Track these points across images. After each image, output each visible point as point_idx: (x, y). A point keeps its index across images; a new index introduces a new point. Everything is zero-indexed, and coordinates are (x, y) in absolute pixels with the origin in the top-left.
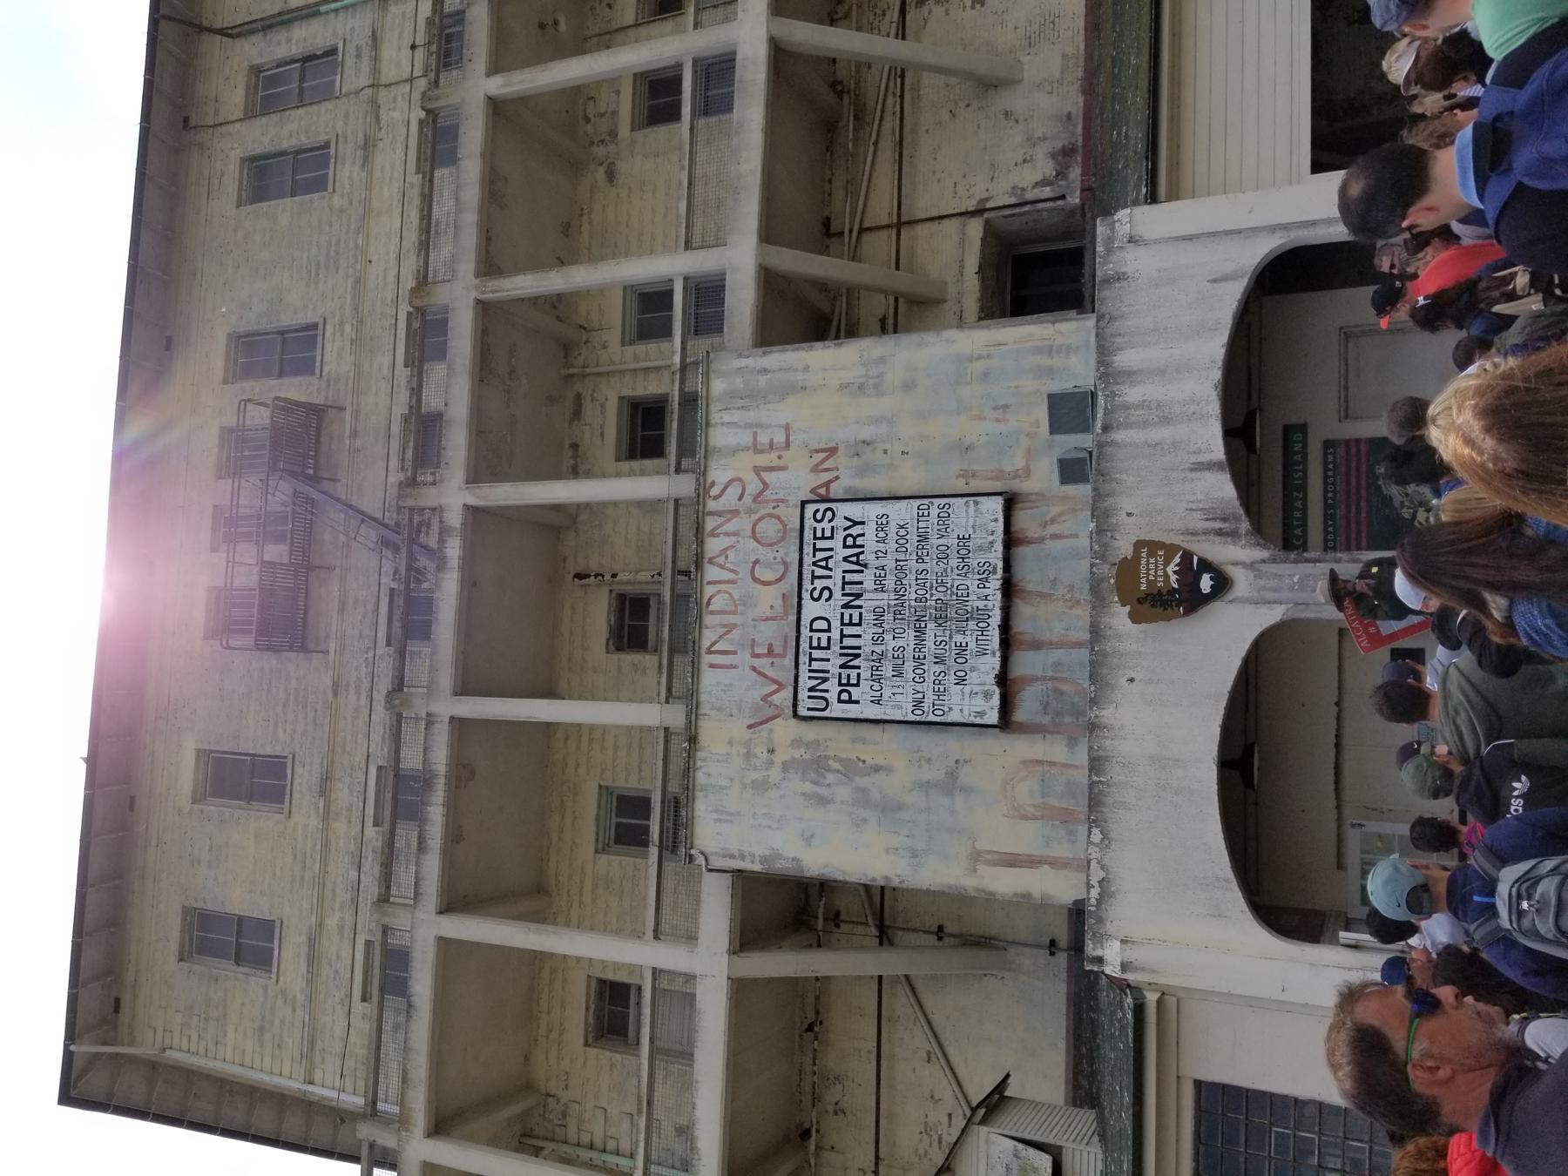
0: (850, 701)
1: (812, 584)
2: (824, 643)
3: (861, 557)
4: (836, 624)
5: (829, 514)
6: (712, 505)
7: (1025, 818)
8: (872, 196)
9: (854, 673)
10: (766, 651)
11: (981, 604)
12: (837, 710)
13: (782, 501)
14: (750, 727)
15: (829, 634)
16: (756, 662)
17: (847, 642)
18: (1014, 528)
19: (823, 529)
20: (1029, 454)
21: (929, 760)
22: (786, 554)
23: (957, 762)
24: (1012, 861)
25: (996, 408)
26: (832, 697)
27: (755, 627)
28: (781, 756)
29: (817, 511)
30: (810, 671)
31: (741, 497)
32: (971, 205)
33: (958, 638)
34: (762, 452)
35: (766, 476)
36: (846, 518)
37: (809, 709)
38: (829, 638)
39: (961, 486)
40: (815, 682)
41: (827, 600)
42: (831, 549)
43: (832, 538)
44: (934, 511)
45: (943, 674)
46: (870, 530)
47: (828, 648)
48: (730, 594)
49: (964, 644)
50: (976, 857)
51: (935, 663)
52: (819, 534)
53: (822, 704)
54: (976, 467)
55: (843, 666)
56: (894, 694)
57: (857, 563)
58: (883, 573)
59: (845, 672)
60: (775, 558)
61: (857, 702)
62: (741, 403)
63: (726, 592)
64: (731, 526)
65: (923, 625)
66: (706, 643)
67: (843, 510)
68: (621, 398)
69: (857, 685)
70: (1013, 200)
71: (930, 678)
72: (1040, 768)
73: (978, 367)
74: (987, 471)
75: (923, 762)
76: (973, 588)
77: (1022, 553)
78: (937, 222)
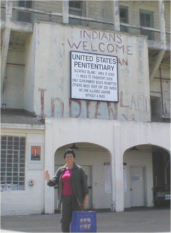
0: (75, 65)
2: (87, 59)
5: (114, 63)
7: (52, 102)
13: (117, 52)
16: (82, 42)
18: (111, 103)
19: (111, 61)
23: (62, 88)
24: (42, 99)
25: (134, 100)
26: (76, 60)
29: (115, 60)
30: (81, 56)
31: (118, 42)
33: (89, 91)
34: (127, 48)
36: (113, 67)
37: (73, 55)
39: (120, 92)
40: (79, 56)
41: (97, 61)
43: (110, 63)
44: (115, 86)
46: (111, 72)
50: (42, 91)
52: (110, 60)
53: (74, 58)
55: (82, 63)
56: (77, 75)
57: (104, 68)
61: (75, 66)
63: (97, 36)
66: (86, 30)
67: (115, 65)
68: (128, 7)
69: (79, 66)
70: (164, 104)
72: (62, 106)
73: (142, 97)
76: (99, 94)
77: (106, 104)
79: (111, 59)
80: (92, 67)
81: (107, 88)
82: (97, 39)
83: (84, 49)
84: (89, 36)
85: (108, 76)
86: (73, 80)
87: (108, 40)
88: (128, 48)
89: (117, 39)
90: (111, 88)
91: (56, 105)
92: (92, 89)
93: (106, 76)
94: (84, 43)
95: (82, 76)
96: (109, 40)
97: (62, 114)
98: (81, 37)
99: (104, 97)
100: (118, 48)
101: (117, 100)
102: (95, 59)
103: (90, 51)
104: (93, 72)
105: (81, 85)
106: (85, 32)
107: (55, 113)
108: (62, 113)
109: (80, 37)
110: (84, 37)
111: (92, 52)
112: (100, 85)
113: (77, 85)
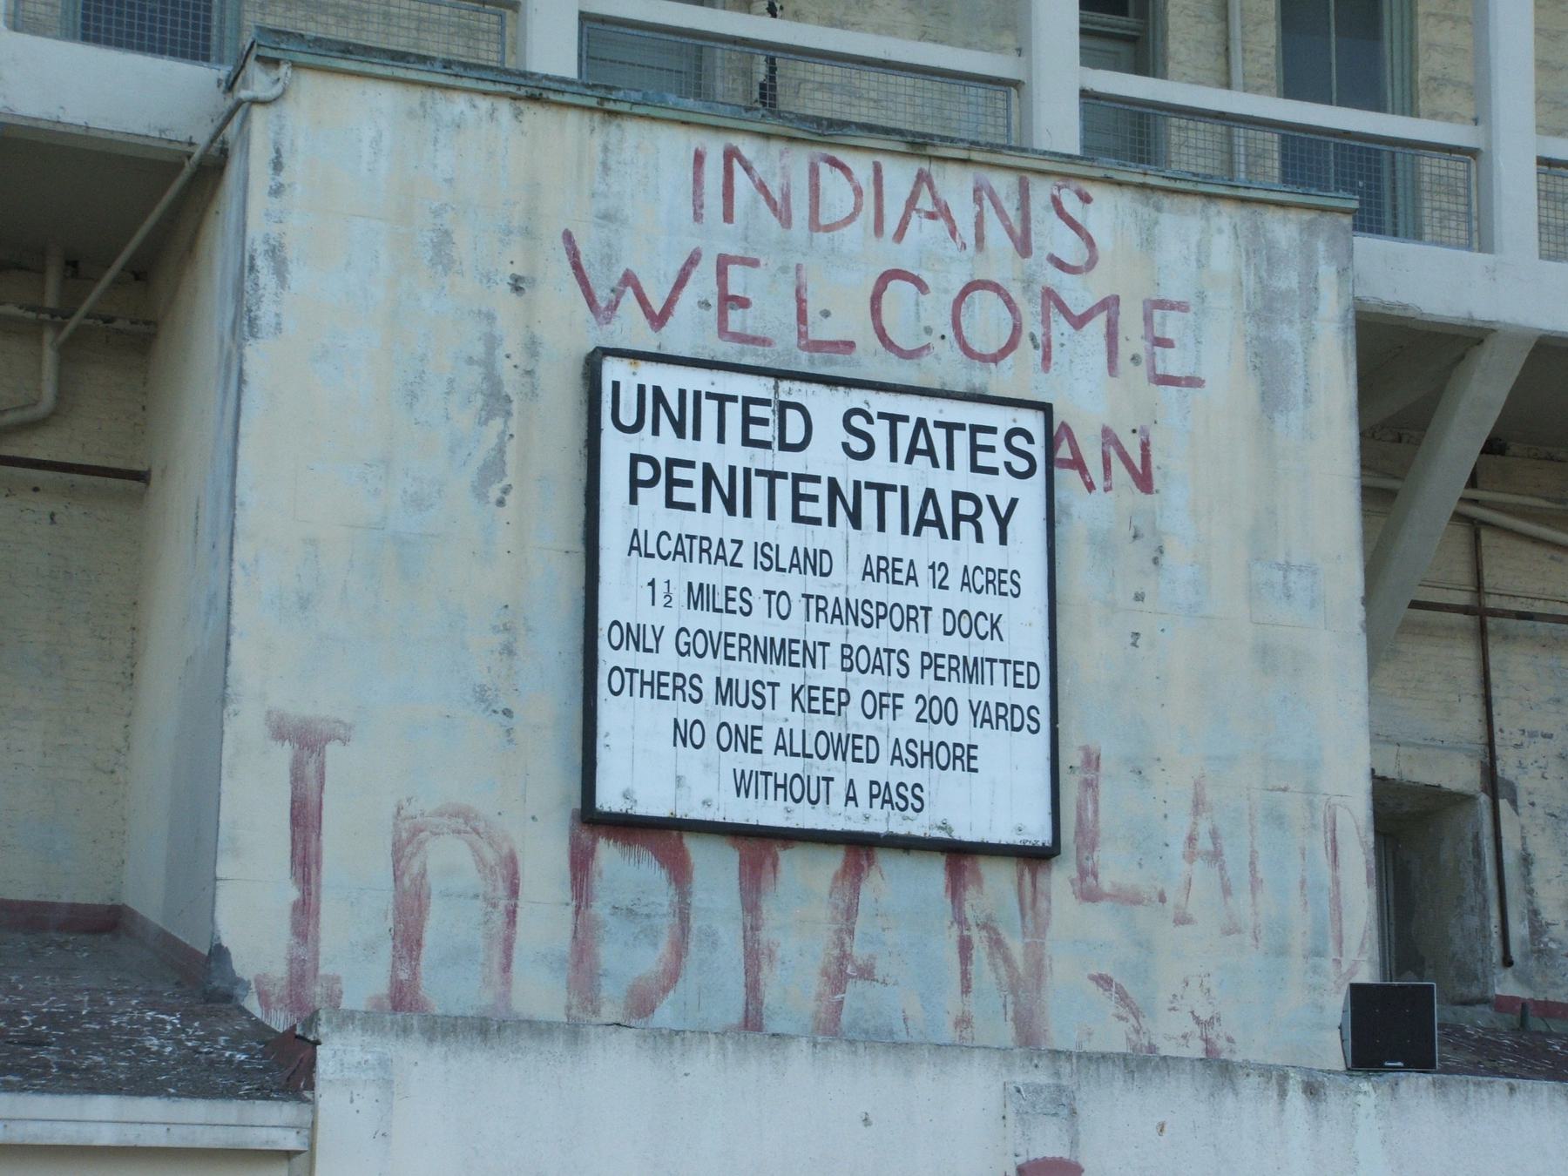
0: (635, 483)
1: (882, 416)
2: (756, 432)
3: (935, 531)
4: (790, 463)
5: (1021, 465)
6: (1041, 191)
8: (1539, 552)
9: (694, 495)
10: (732, 291)
11: (838, 788)
12: (616, 449)
13: (1047, 358)
14: (568, 237)
15: (776, 445)
16: (707, 268)
17: (760, 485)
19: (991, 449)
20: (1129, 898)
21: (509, 650)
22: (938, 358)
23: (507, 713)
25: (1214, 835)
27: (784, 269)
28: (504, 303)
29: (1030, 440)
30: (697, 394)
31: (1061, 265)
32: (1507, 767)
34: (1148, 319)
35: (1098, 324)
36: (1014, 502)
37: (616, 385)
38: (766, 445)
39: (1070, 756)
41: (846, 446)
42: (950, 466)
43: (975, 468)
44: (1024, 698)
45: (696, 695)
46: (990, 554)
47: (747, 441)
48: (851, 219)
49: (757, 745)
51: (718, 679)
52: (982, 439)
53: (628, 418)
54: (1105, 788)
55: (709, 473)
56: (652, 584)
57: (922, 522)
58: (900, 577)
59: (696, 475)
60: (928, 330)
61: (634, 500)
62: (1250, 282)
63: (857, 208)
64: (995, 231)
65: (796, 659)
66: (748, 147)
67: (1031, 493)
69: (670, 503)
70: (1510, 858)
71: (689, 666)
72: (502, 892)
74: (1096, 812)
75: (502, 638)
78: (1479, 691)
79: (993, 430)
80: (806, 509)
81: (935, 710)
82: (855, 236)
83: (723, 329)
84: (777, 196)
85: (958, 599)
86: (616, 641)
87: (964, 246)
88: (1157, 314)
89: (1053, 237)
90: (985, 716)
91: (435, 883)
92: (797, 721)
93: (938, 601)
94: (722, 272)
95: (699, 596)
96: (970, 240)
97: (497, 977)
98: (698, 217)
99: (912, 799)
100: (1060, 325)
101: (1042, 836)
102: (829, 433)
103: (786, 351)
104: (813, 562)
105: (688, 686)
106: (736, 164)
107: (428, 954)
108: (497, 957)
109: (689, 210)
110: (728, 216)
111: (804, 355)
112: (876, 682)
113: (655, 685)
